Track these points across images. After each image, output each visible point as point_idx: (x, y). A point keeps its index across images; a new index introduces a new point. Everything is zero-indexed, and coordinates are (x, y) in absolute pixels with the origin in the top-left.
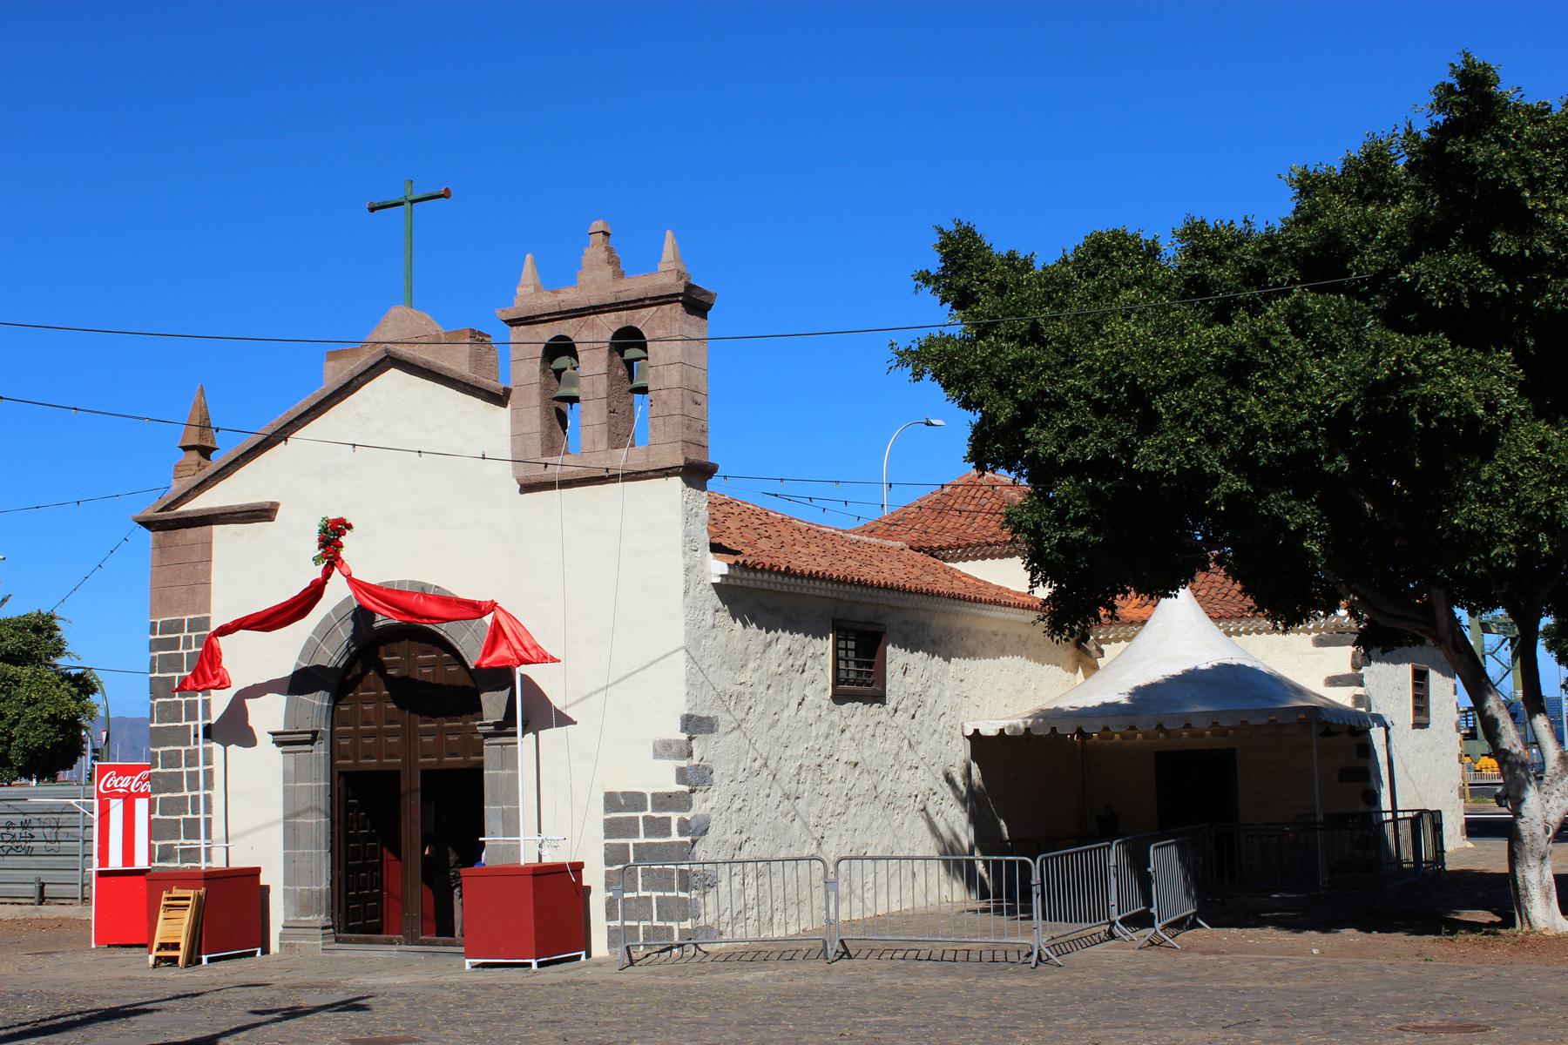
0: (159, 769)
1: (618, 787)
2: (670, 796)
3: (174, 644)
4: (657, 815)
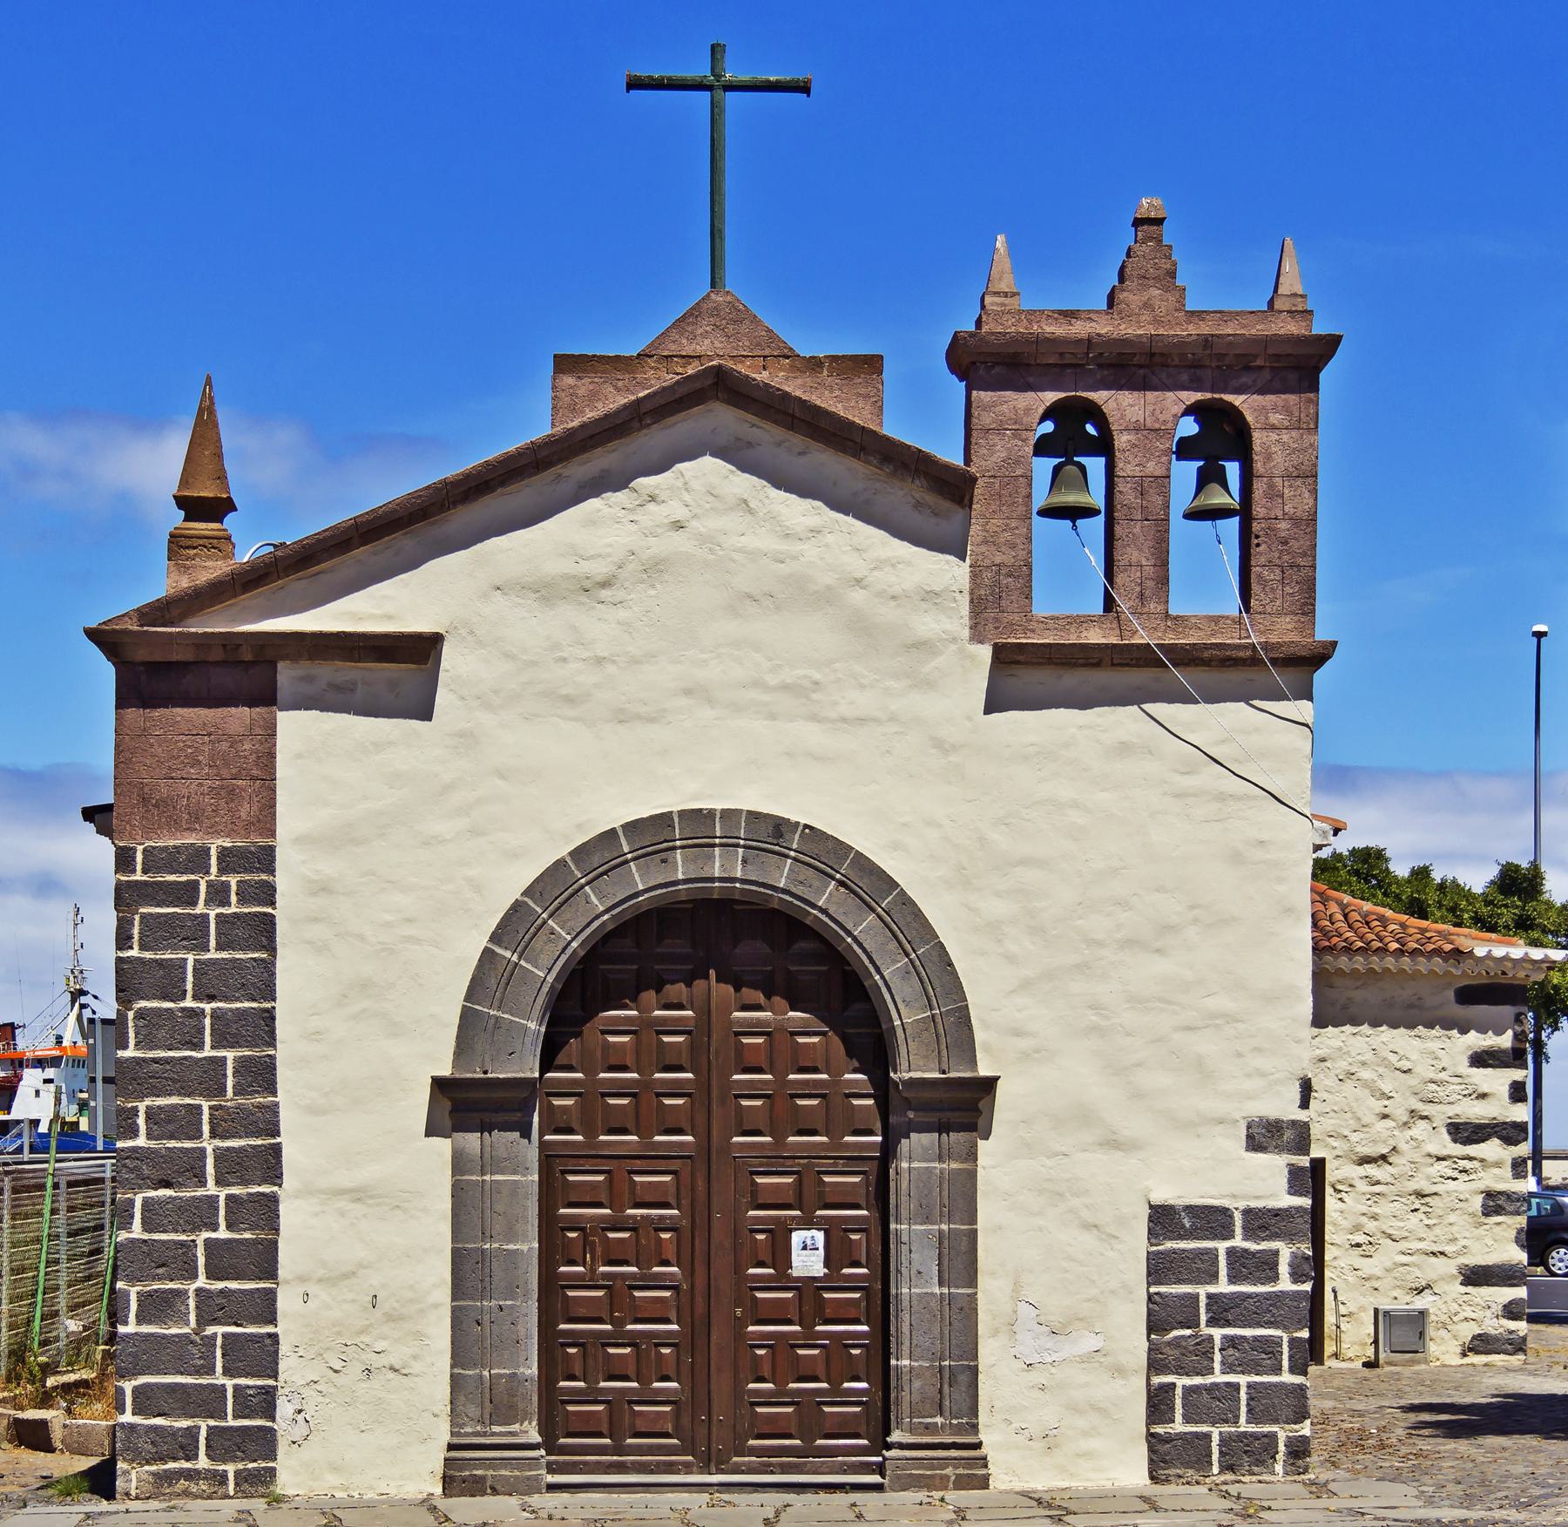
0: (141, 1141)
1: (1168, 1193)
2: (1276, 1213)
3: (187, 894)
4: (1252, 1246)
